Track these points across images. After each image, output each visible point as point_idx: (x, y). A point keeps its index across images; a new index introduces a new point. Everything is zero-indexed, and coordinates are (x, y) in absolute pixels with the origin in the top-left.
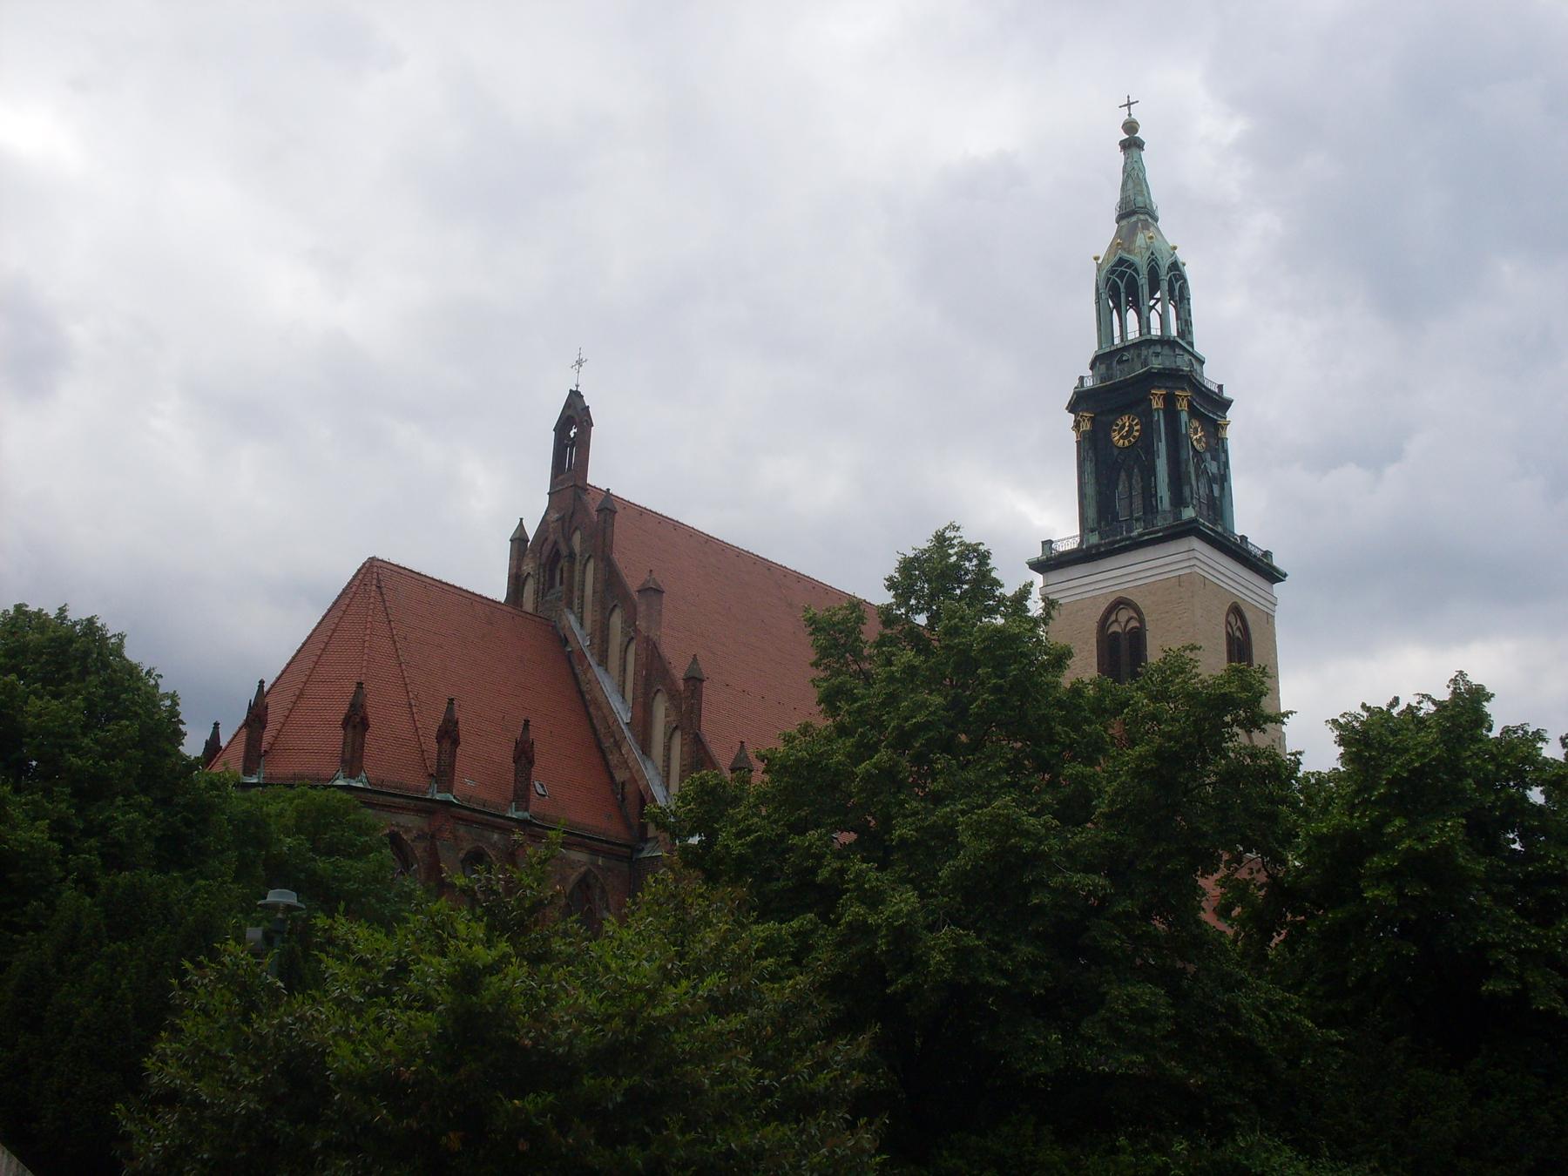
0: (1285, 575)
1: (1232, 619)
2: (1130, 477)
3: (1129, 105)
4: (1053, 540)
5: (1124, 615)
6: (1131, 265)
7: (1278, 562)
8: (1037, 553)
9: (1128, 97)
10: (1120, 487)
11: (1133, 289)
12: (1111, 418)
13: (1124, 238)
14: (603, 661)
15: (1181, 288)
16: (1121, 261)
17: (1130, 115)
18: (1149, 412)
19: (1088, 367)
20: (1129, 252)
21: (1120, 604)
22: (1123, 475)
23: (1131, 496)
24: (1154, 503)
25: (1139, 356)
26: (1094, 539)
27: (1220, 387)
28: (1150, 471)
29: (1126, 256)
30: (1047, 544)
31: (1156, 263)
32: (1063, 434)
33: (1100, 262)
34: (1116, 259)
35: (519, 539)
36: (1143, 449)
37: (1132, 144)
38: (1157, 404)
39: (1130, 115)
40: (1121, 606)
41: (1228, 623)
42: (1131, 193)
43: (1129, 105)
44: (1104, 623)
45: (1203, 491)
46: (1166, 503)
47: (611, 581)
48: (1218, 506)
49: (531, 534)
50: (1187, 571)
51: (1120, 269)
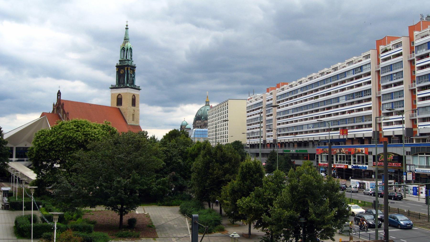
1: (133, 96)
2: (122, 77)
3: (127, 22)
5: (120, 96)
6: (125, 48)
7: (140, 88)
13: (125, 43)
14: (63, 119)
16: (123, 47)
20: (125, 46)
21: (119, 94)
22: (121, 77)
26: (117, 86)
32: (115, 70)
35: (54, 105)
36: (123, 75)
37: (127, 29)
38: (126, 69)
41: (132, 97)
44: (118, 96)
45: (131, 79)
46: (126, 82)
47: (64, 112)
48: (133, 82)
49: (55, 104)
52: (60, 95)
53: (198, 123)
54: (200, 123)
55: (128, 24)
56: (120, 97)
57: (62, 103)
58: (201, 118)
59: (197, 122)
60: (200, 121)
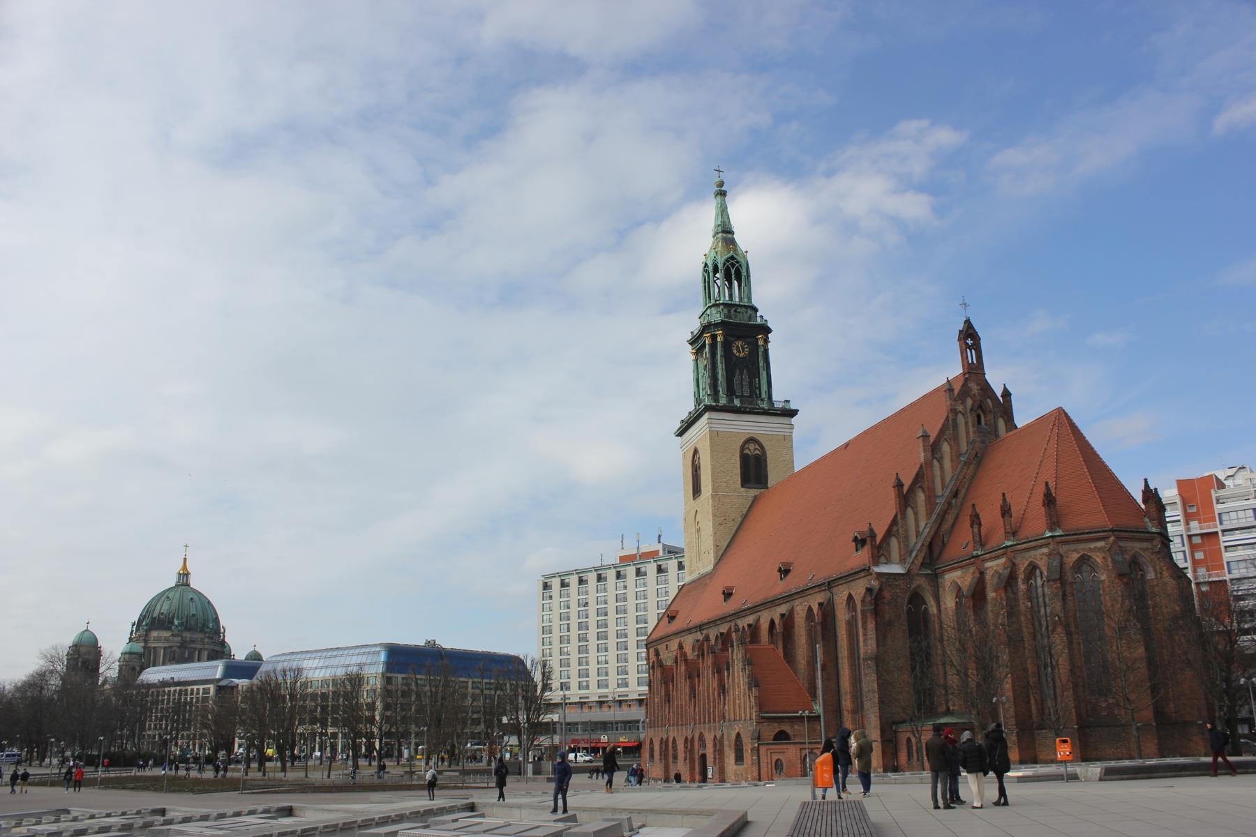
2: (741, 374)
5: (752, 446)
6: (738, 262)
10: (736, 377)
12: (732, 339)
16: (732, 258)
18: (758, 346)
21: (752, 440)
22: (738, 372)
23: (742, 385)
24: (758, 392)
25: (746, 312)
28: (755, 374)
29: (735, 256)
34: (729, 255)
42: (726, 220)
44: (742, 448)
50: (789, 434)
52: (977, 347)
53: (158, 639)
54: (167, 640)
55: (724, 177)
56: (752, 449)
57: (999, 392)
58: (172, 622)
59: (154, 634)
60: (166, 634)
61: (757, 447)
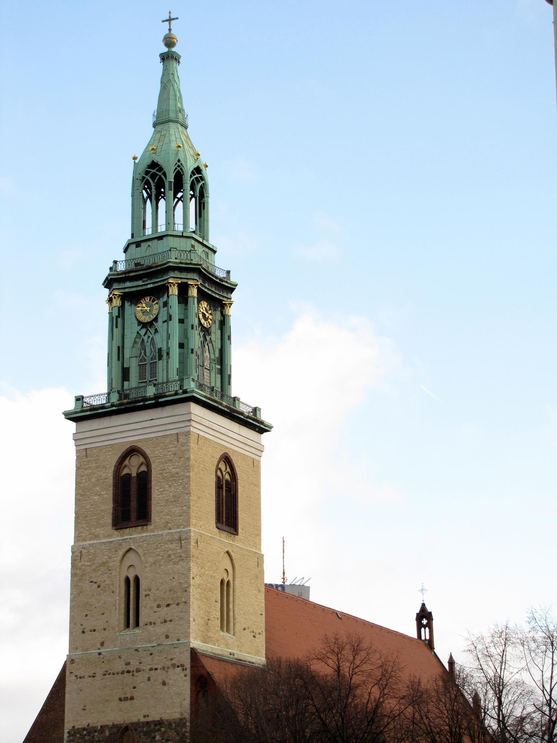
0: (271, 427)
1: (222, 466)
3: (170, 20)
4: (85, 395)
6: (161, 169)
7: (265, 417)
8: (71, 406)
9: (170, 13)
11: (160, 184)
15: (202, 188)
16: (154, 165)
17: (170, 30)
19: (122, 250)
27: (228, 272)
30: (79, 399)
31: (181, 169)
33: (137, 161)
39: (170, 30)
40: (135, 453)
41: (218, 469)
43: (170, 20)
51: (153, 171)
61: (142, 459)
